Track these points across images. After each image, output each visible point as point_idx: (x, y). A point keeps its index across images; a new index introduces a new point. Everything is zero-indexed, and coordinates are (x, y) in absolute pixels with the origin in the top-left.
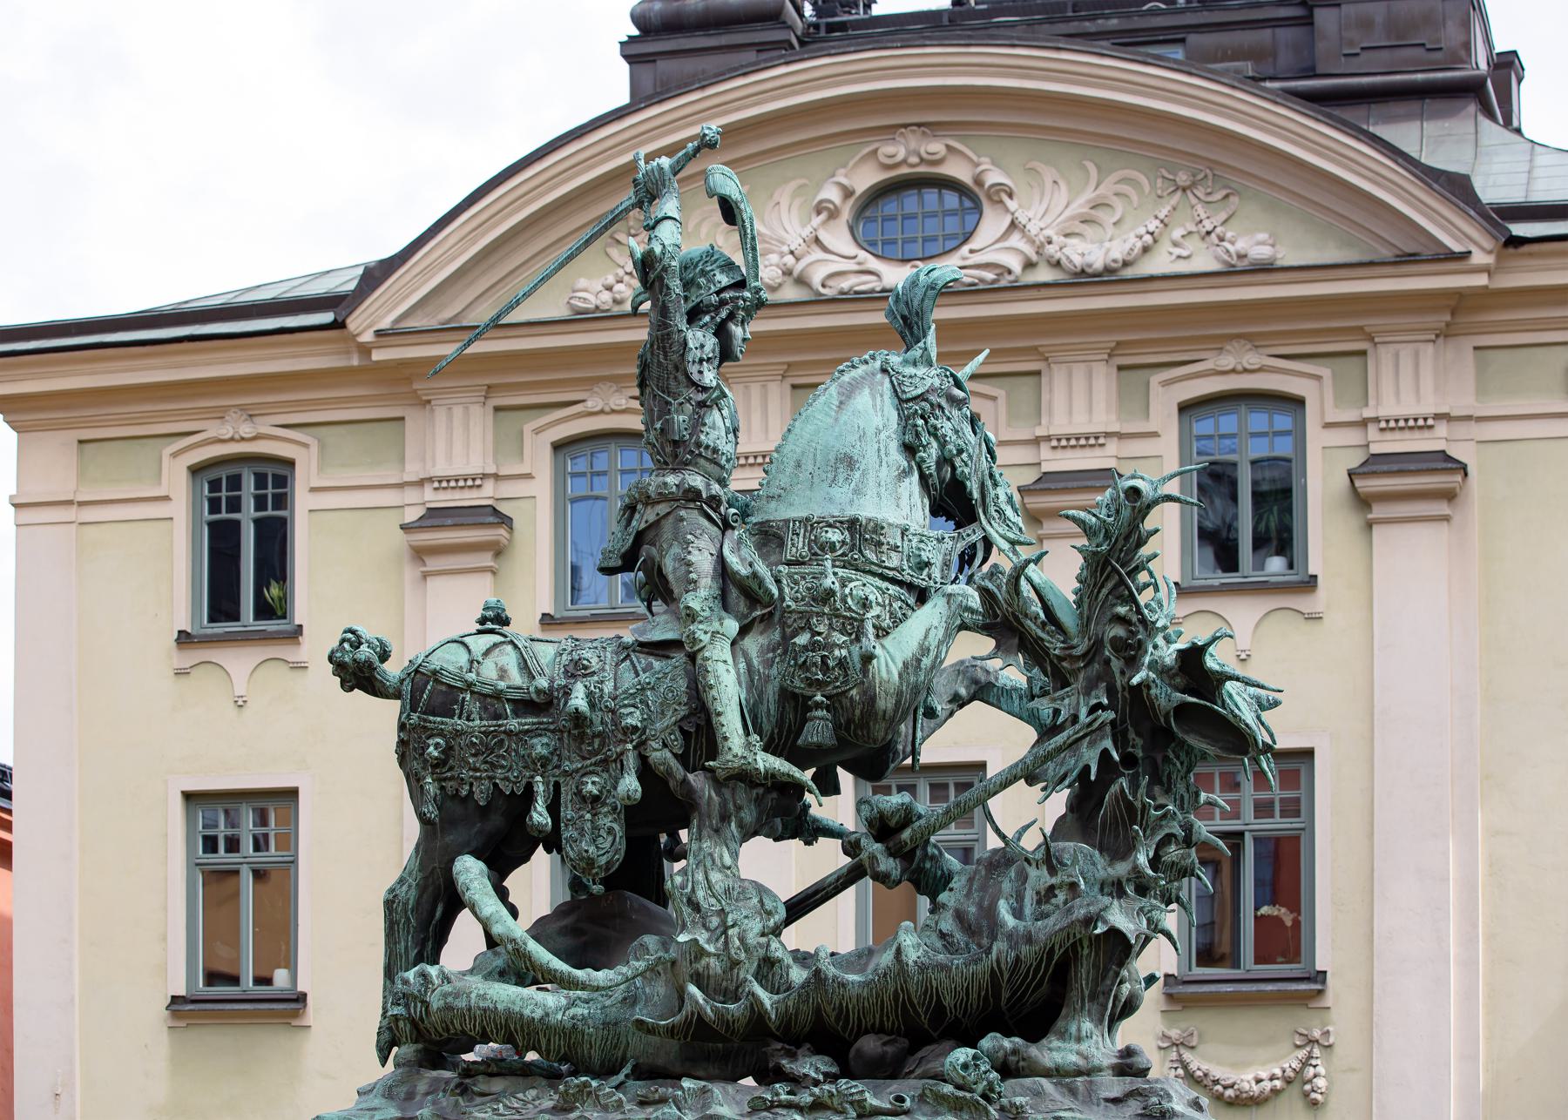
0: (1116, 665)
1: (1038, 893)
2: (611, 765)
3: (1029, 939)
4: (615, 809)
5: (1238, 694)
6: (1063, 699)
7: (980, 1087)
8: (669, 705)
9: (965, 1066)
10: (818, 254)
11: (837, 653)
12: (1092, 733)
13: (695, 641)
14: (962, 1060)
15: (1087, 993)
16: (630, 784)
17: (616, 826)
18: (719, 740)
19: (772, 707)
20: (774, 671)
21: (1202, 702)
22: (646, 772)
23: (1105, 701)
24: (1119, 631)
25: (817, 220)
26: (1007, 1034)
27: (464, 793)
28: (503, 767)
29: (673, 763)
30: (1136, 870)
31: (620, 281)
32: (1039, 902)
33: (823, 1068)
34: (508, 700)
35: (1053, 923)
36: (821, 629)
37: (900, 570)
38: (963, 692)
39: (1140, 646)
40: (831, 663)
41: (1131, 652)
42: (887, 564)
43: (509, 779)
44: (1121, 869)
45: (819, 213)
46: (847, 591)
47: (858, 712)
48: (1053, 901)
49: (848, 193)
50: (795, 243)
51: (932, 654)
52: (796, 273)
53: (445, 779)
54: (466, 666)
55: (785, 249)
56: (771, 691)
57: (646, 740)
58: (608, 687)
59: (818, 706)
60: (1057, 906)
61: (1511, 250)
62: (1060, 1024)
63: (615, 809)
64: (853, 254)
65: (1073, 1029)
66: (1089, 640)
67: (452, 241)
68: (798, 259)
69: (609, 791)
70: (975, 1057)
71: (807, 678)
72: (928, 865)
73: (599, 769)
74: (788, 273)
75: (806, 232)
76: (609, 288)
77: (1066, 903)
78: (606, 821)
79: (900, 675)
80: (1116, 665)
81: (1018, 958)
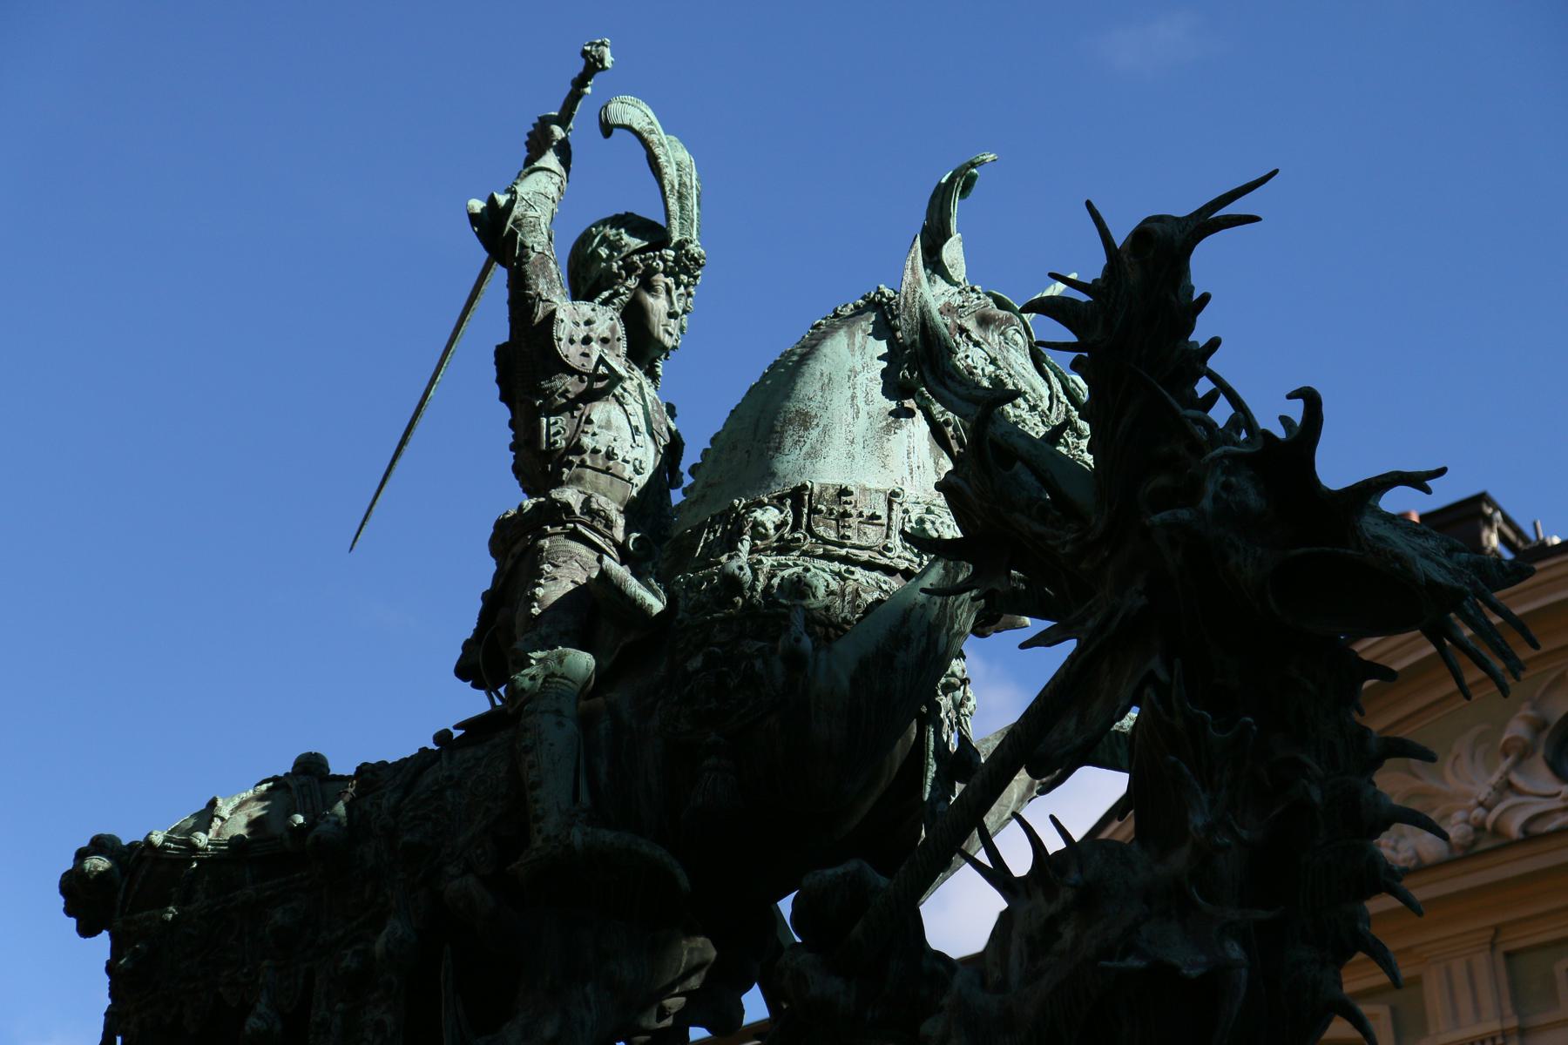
5: (1426, 556)
10: (1512, 800)
21: (1315, 549)
25: (1505, 765)
42: (855, 541)
45: (1506, 756)
49: (1538, 726)
50: (1483, 791)
52: (1489, 825)
55: (1472, 802)
64: (1556, 791)
68: (1489, 809)
74: (1479, 828)
75: (1495, 778)
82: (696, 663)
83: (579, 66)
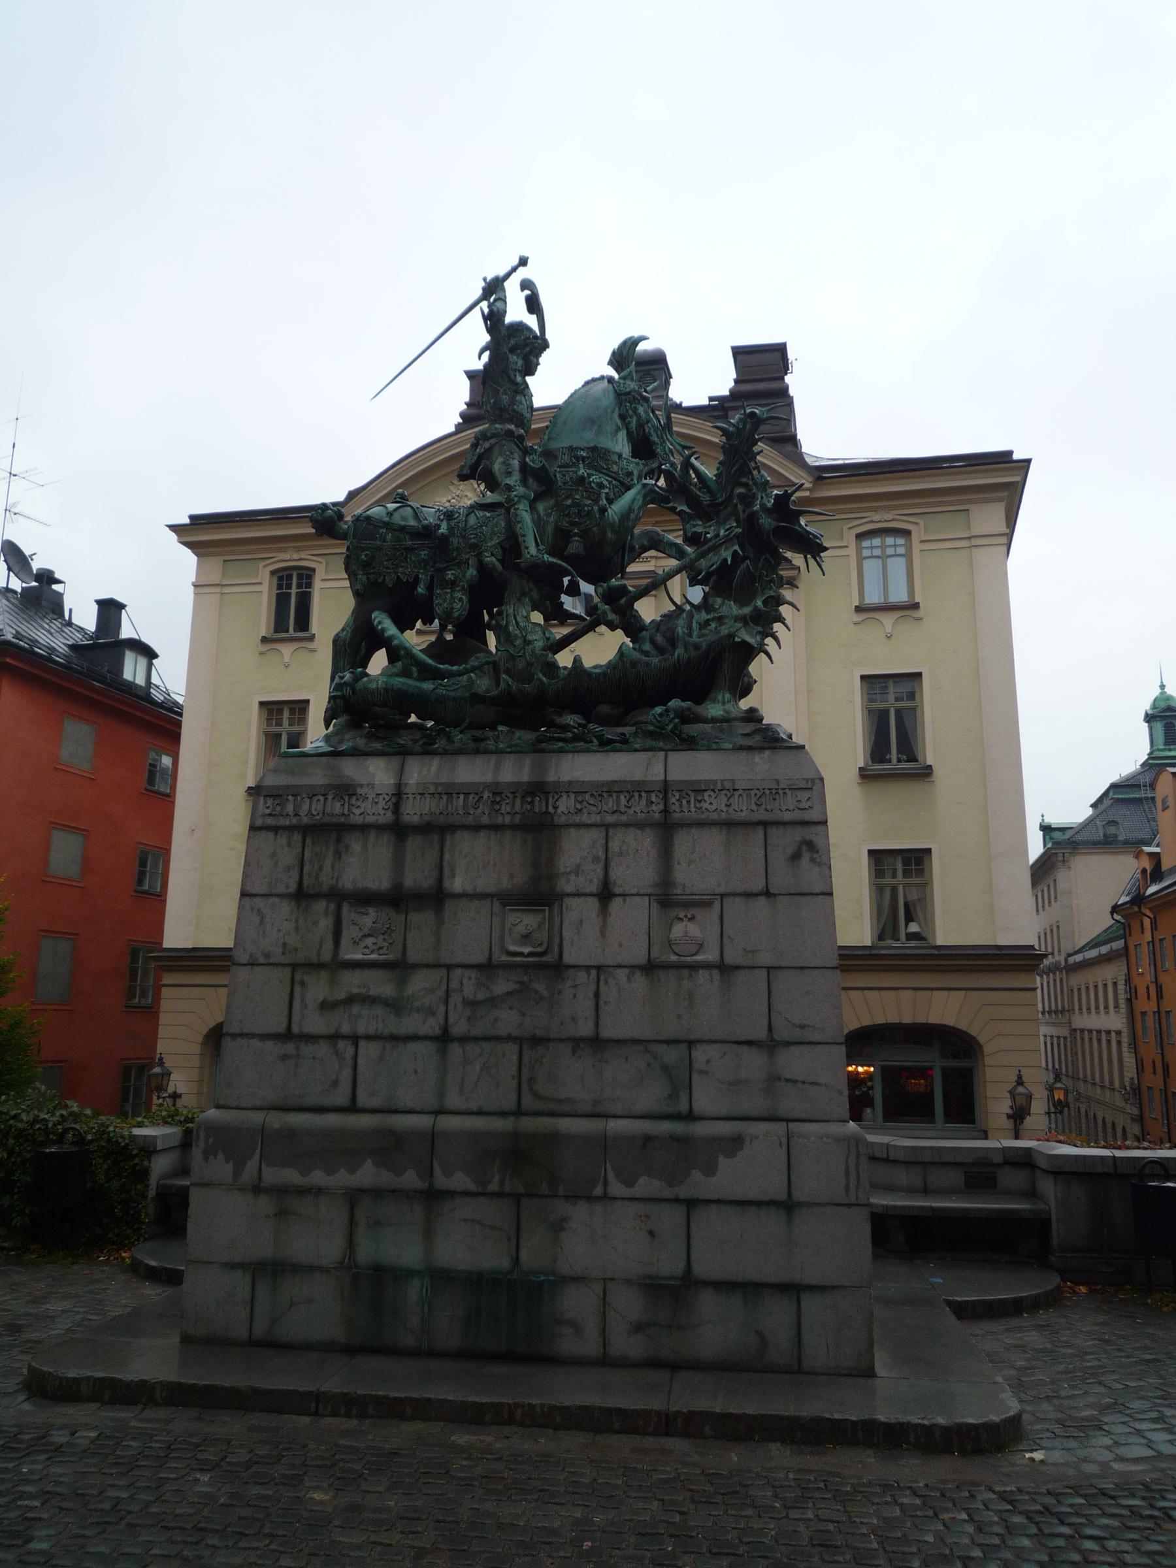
0: (740, 507)
1: (700, 624)
2: (462, 565)
3: (697, 646)
4: (463, 588)
6: (711, 526)
7: (670, 727)
8: (495, 534)
9: (661, 715)
11: (586, 508)
12: (728, 540)
13: (509, 500)
14: (658, 712)
15: (727, 678)
16: (472, 572)
17: (464, 597)
18: (522, 548)
19: (550, 537)
20: (552, 519)
22: (482, 567)
23: (735, 524)
24: (742, 490)
26: (683, 701)
27: (380, 581)
28: (402, 567)
29: (497, 563)
30: (756, 608)
31: (454, 498)
32: (700, 629)
33: (580, 721)
34: (407, 533)
35: (711, 638)
36: (577, 497)
37: (615, 473)
38: (646, 543)
39: (754, 496)
40: (583, 514)
41: (748, 500)
43: (406, 571)
44: (746, 610)
46: (591, 479)
47: (597, 539)
48: (709, 627)
51: (636, 513)
53: (371, 573)
54: (385, 515)
56: (550, 529)
57: (483, 551)
58: (462, 525)
59: (576, 535)
60: (711, 630)
61: (819, 482)
62: (712, 695)
63: (463, 588)
65: (720, 697)
66: (726, 493)
67: (385, 481)
69: (460, 579)
70: (667, 711)
71: (570, 521)
72: (633, 620)
73: (456, 567)
76: (449, 501)
77: (716, 628)
78: (459, 595)
79: (619, 521)
80: (740, 507)
81: (689, 658)
82: (569, 502)
83: (516, 262)
